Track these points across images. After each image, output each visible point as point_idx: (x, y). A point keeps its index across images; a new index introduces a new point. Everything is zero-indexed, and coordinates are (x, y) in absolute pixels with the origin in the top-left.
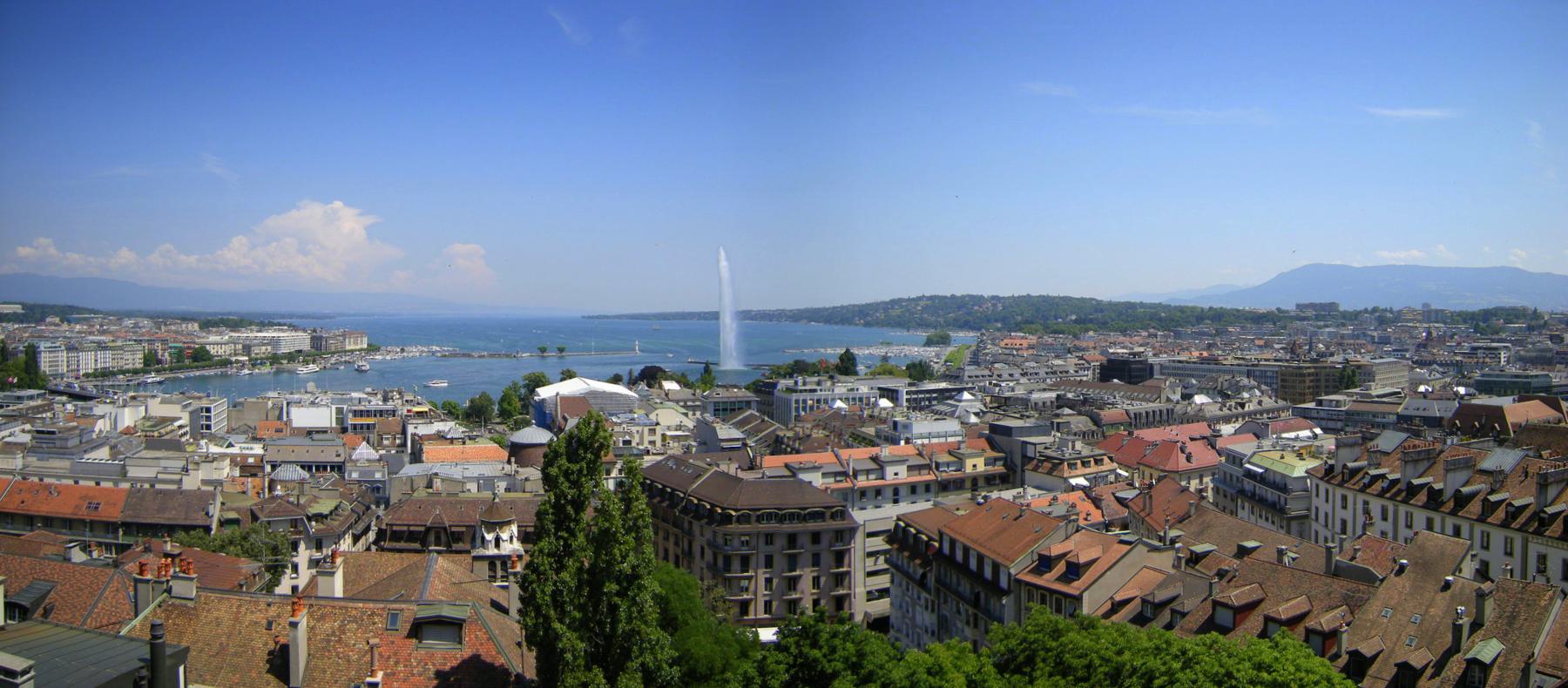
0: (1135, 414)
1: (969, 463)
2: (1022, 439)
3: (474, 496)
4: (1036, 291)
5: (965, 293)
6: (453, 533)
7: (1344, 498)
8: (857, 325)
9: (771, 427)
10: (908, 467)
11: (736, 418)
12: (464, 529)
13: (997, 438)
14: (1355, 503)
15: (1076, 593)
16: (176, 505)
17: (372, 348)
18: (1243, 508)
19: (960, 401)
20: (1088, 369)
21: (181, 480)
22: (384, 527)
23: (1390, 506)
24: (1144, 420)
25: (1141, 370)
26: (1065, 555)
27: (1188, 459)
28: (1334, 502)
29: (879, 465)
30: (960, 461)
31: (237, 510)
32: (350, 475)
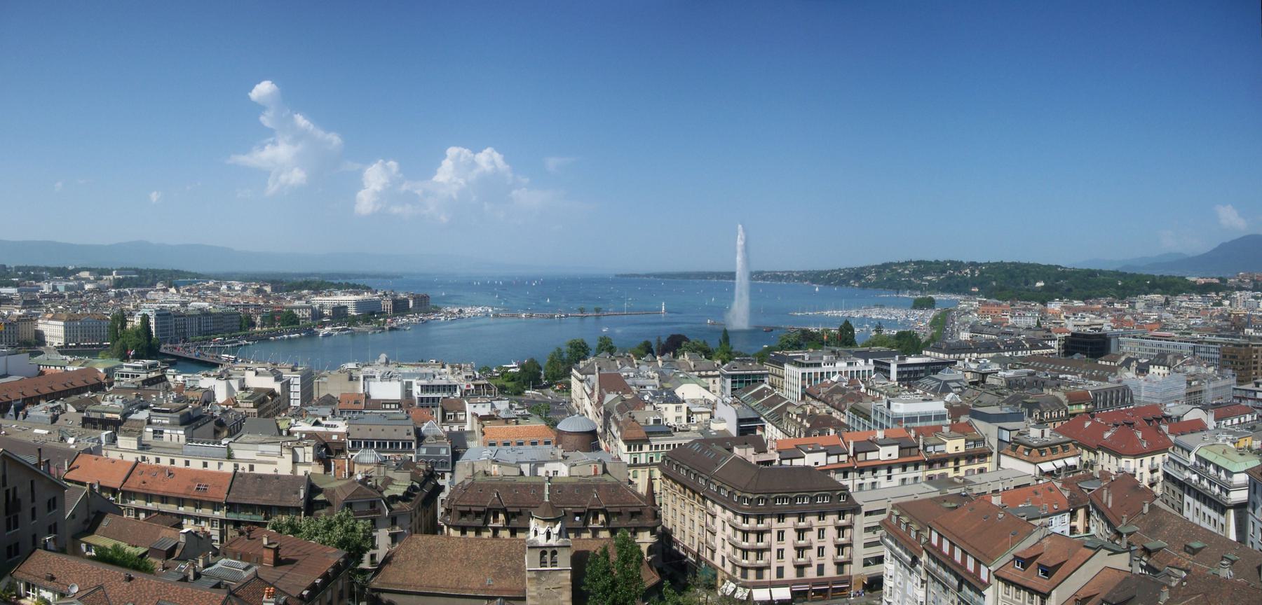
3: (527, 480)
4: (1008, 259)
5: (947, 259)
9: (781, 402)
11: (750, 391)
16: (273, 488)
26: (1036, 557)
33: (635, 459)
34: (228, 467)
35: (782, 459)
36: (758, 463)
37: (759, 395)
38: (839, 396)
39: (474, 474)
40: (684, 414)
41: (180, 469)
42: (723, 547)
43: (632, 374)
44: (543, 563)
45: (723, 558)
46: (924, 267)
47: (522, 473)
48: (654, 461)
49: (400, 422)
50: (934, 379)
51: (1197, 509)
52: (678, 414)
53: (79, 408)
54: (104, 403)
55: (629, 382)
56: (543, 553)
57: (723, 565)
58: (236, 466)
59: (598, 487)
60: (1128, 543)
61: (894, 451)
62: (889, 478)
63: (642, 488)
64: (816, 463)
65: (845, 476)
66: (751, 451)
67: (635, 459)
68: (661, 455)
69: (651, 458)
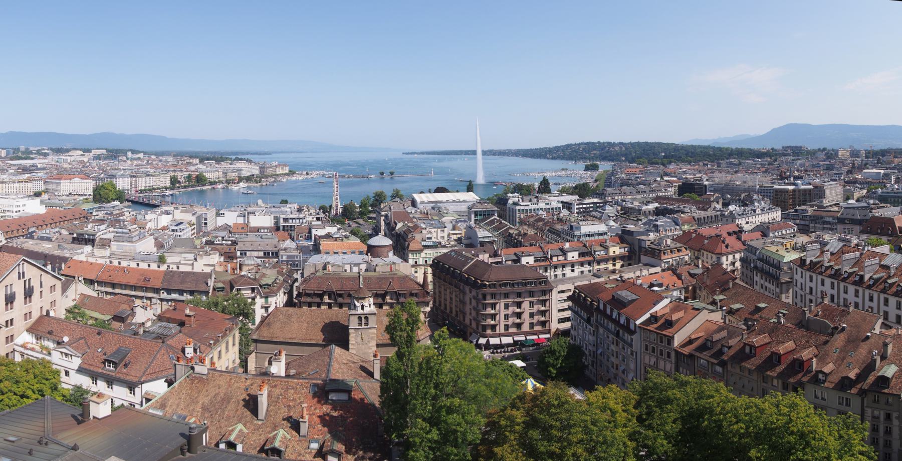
0: (698, 219)
1: (611, 250)
2: (639, 237)
4: (642, 140)
6: (337, 294)
7: (811, 277)
8: (548, 158)
10: (579, 254)
12: (343, 292)
13: (626, 237)
14: (817, 280)
15: (671, 335)
17: (291, 173)
18: (757, 275)
19: (605, 210)
20: (672, 187)
21: (193, 264)
22: (301, 291)
23: (836, 282)
24: (702, 221)
25: (701, 188)
26: (664, 315)
27: (727, 247)
28: (805, 278)
29: (564, 252)
30: (606, 249)
31: (223, 282)
32: (282, 258)
33: (416, 262)
34: (164, 268)
35: (506, 261)
36: (491, 263)
37: (493, 222)
38: (540, 223)
39: (316, 272)
40: (445, 235)
41: (133, 268)
42: (471, 314)
43: (413, 212)
44: (360, 324)
45: (470, 320)
46: (590, 146)
47: (345, 270)
48: (428, 263)
49: (270, 240)
50: (599, 212)
51: (762, 285)
52: (443, 235)
53: (70, 232)
54: (86, 229)
55: (411, 216)
56: (360, 318)
57: (471, 324)
58: (169, 266)
59: (393, 278)
60: (720, 306)
61: (576, 255)
62: (573, 271)
63: (420, 280)
64: (528, 263)
65: (546, 271)
66: (487, 256)
67: (416, 262)
68: (432, 259)
69: (426, 261)
